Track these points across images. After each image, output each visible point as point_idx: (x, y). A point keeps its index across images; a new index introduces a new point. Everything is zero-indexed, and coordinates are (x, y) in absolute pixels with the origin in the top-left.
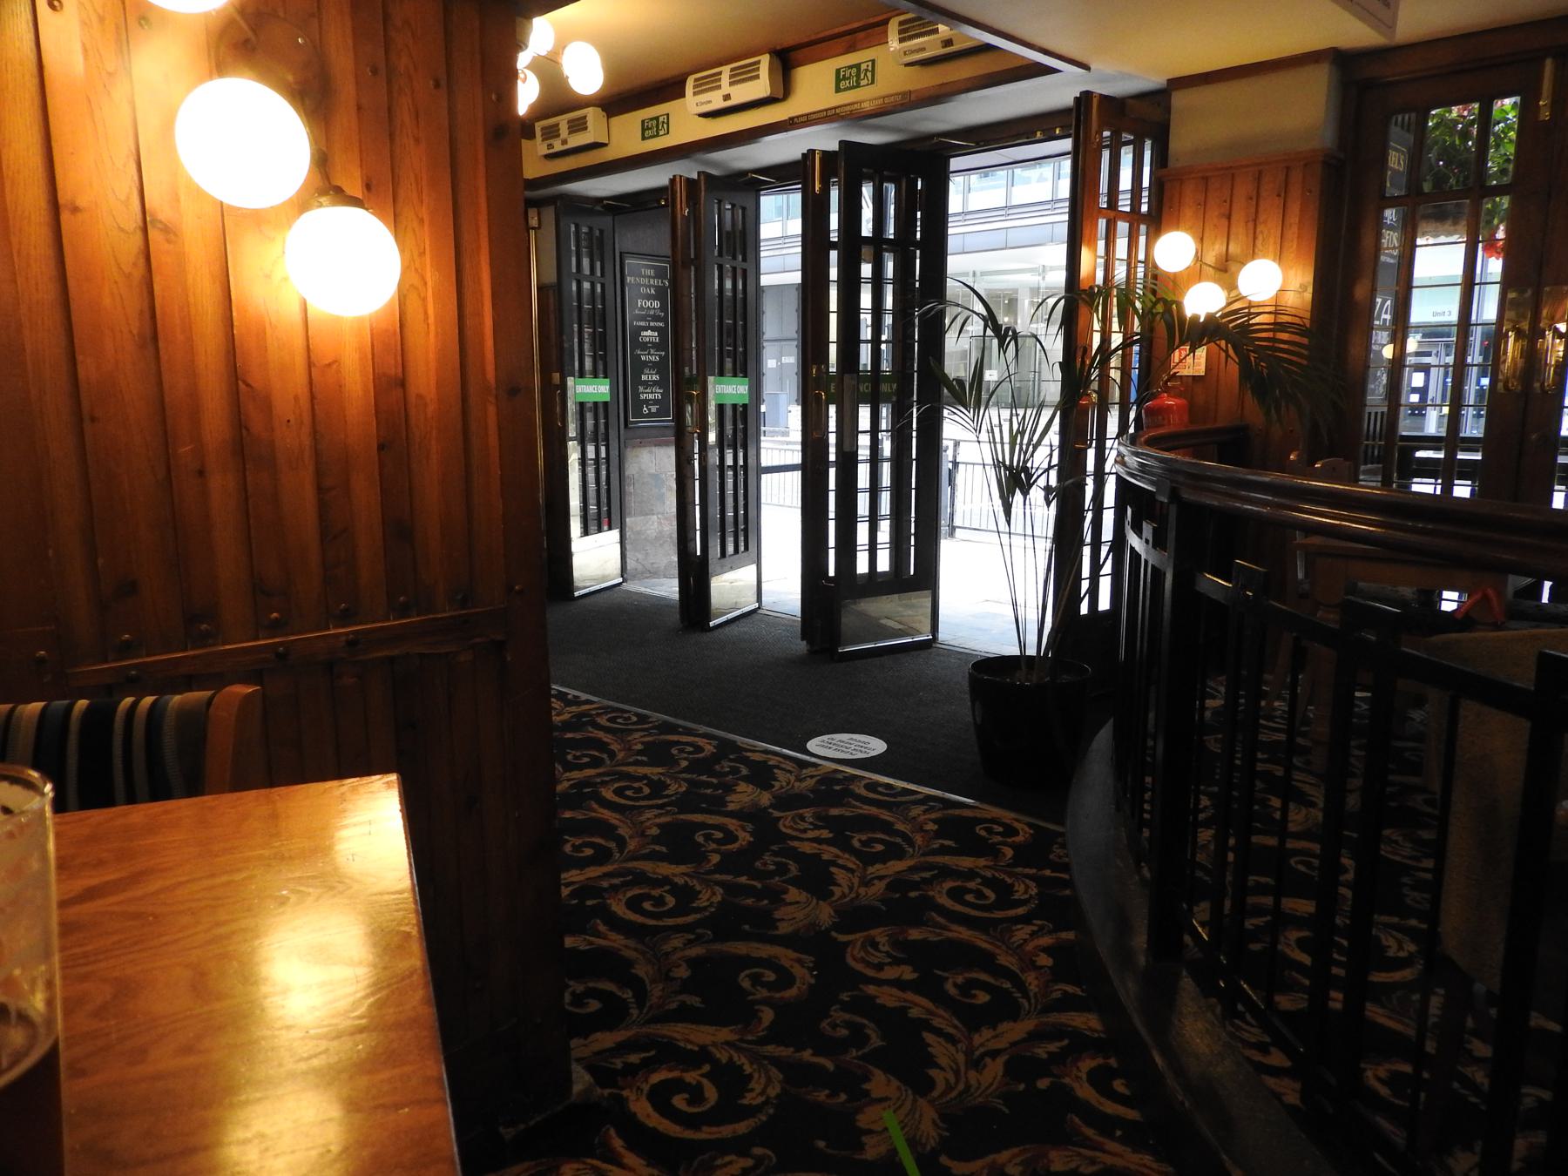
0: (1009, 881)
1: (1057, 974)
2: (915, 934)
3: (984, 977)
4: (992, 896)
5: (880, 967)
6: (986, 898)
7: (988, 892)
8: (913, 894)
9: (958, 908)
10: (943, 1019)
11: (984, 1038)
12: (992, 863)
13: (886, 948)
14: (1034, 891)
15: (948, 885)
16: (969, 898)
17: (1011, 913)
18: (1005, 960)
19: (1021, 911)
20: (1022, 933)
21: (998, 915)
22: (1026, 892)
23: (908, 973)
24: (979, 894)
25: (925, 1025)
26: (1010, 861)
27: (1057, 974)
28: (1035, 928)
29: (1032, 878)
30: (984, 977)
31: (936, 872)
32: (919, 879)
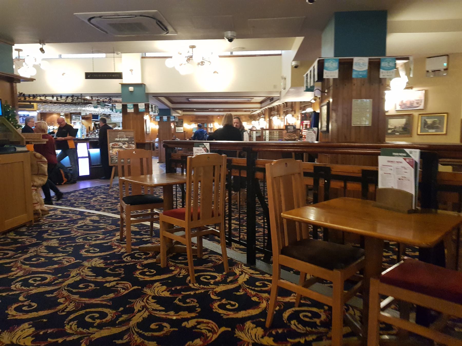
0: (80, 329)
1: (56, 298)
2: (112, 295)
3: (84, 290)
4: (87, 319)
5: (117, 284)
6: (90, 317)
7: (90, 320)
8: (121, 309)
9: (100, 309)
10: (93, 279)
11: (78, 278)
12: (91, 336)
13: (119, 289)
14: (67, 327)
15: (109, 318)
16: (97, 315)
17: (77, 314)
18: (76, 297)
19: (72, 316)
20: (71, 307)
21: (83, 312)
22: (71, 326)
23: (108, 285)
24: (93, 318)
25: (96, 276)
26: (81, 341)
27: (56, 298)
28: (65, 311)
29: (69, 335)
30: (84, 290)
31: (117, 322)
32: (123, 316)
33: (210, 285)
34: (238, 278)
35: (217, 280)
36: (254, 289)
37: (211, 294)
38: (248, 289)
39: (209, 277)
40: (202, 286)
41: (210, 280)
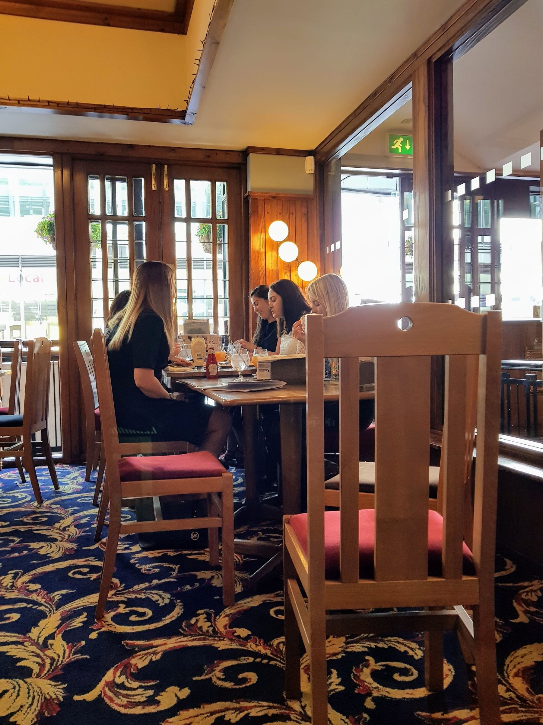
33: (126, 600)
34: (58, 627)
35: (112, 614)
36: (28, 604)
37: (119, 585)
38: (43, 601)
39: (133, 618)
40: (143, 596)
41: (127, 610)
